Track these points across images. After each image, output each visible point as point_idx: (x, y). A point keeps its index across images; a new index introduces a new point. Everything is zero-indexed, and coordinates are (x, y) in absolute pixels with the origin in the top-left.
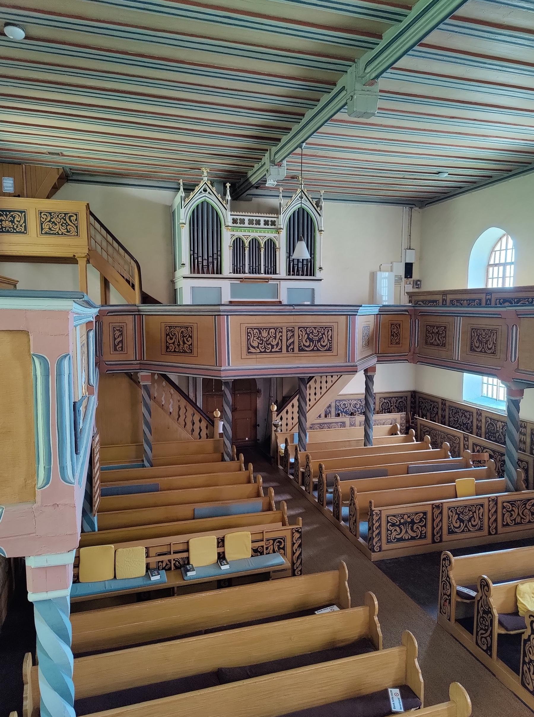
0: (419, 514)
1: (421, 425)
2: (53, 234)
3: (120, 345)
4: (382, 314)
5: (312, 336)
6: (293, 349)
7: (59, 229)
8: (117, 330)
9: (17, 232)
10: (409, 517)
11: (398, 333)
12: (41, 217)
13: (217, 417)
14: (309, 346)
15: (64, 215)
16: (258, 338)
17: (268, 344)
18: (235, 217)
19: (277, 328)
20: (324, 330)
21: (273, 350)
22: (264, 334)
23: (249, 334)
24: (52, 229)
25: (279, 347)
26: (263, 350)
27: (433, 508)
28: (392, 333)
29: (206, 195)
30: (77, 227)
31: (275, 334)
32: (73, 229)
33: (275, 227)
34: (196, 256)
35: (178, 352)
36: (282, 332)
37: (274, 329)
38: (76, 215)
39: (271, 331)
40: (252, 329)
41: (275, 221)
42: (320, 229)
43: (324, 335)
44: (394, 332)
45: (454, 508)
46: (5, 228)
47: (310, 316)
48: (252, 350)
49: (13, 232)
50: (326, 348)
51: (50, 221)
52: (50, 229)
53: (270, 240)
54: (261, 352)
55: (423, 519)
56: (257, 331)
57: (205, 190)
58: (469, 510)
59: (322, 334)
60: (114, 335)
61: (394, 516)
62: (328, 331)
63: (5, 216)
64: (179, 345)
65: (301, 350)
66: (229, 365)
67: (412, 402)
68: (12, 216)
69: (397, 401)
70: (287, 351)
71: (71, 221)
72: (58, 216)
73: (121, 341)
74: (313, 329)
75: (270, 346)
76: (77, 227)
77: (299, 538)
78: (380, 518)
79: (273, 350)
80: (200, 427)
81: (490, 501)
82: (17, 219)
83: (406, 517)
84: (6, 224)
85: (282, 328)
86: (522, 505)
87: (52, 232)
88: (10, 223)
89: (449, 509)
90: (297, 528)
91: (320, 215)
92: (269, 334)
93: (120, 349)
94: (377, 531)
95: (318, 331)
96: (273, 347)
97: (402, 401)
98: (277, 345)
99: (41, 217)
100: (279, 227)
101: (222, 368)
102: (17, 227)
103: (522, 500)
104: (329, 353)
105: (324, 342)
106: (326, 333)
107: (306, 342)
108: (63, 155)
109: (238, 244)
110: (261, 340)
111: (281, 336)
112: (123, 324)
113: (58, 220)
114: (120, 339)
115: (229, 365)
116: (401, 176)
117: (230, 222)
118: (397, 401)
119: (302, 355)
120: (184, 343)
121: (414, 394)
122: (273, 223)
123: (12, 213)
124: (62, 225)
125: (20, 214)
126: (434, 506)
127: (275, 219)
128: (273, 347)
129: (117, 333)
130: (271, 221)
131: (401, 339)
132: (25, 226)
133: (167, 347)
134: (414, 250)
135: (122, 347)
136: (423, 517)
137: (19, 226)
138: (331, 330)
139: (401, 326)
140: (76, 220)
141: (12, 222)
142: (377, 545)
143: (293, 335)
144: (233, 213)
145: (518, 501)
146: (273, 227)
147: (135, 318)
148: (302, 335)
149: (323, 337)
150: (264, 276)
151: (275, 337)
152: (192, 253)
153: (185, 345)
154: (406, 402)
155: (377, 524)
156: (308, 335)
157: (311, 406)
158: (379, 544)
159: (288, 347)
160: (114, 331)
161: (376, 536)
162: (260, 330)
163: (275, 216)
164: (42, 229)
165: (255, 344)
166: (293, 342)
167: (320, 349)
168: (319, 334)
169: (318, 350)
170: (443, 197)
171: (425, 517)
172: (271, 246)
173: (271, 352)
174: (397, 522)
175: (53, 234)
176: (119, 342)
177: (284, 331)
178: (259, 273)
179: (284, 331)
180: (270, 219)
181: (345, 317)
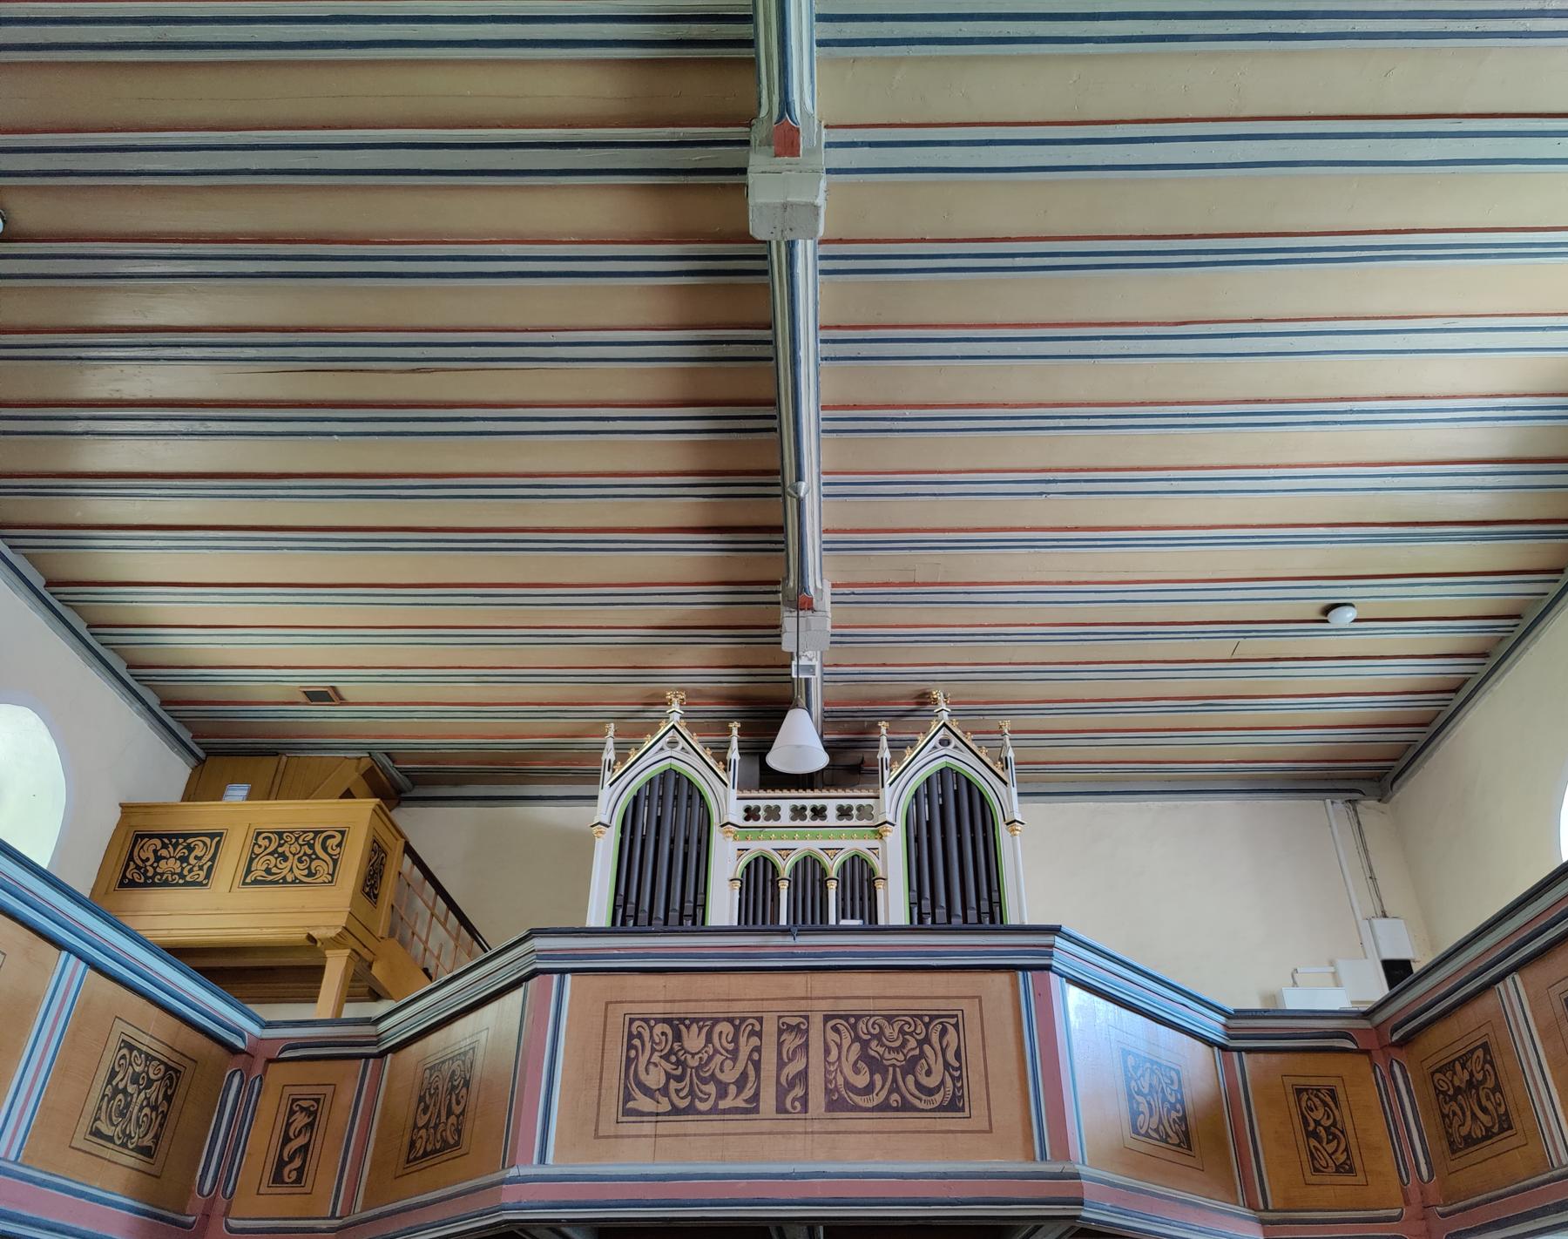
4: (1249, 1050)
6: (804, 1100)
8: (302, 1109)
9: (187, 884)
14: (869, 1089)
16: (666, 1058)
17: (705, 1081)
19: (743, 1020)
21: (723, 1105)
22: (694, 1041)
23: (636, 1042)
24: (274, 870)
25: (748, 1092)
30: (335, 862)
31: (735, 1040)
32: (323, 868)
36: (759, 1035)
37: (730, 1020)
38: (343, 833)
39: (718, 1029)
40: (646, 1021)
43: (926, 1047)
48: (642, 1102)
49: (177, 885)
50: (938, 1098)
51: (275, 851)
54: (675, 1111)
59: (920, 1043)
62: (944, 1032)
63: (171, 849)
70: (781, 1109)
71: (325, 848)
72: (297, 839)
73: (305, 1149)
75: (711, 1088)
79: (723, 1105)
88: (178, 863)
92: (709, 1040)
93: (294, 1175)
95: (901, 1031)
98: (741, 1082)
105: (929, 1073)
106: (935, 1038)
107: (857, 1071)
110: (678, 1063)
111: (758, 1049)
114: (301, 1141)
115: (542, 1160)
120: (450, 1113)
125: (207, 840)
129: (301, 1120)
132: (210, 869)
135: (300, 1170)
138: (956, 1026)
140: (339, 845)
141: (184, 859)
148: (839, 1047)
149: (922, 1055)
151: (734, 1054)
156: (865, 1045)
160: (292, 1113)
162: (677, 1025)
164: (249, 871)
165: (655, 1079)
167: (916, 1102)
169: (906, 1106)
170: (1422, 738)
173: (714, 1110)
175: (271, 882)
177: (770, 1028)
179: (770, 1028)
181: (1003, 979)
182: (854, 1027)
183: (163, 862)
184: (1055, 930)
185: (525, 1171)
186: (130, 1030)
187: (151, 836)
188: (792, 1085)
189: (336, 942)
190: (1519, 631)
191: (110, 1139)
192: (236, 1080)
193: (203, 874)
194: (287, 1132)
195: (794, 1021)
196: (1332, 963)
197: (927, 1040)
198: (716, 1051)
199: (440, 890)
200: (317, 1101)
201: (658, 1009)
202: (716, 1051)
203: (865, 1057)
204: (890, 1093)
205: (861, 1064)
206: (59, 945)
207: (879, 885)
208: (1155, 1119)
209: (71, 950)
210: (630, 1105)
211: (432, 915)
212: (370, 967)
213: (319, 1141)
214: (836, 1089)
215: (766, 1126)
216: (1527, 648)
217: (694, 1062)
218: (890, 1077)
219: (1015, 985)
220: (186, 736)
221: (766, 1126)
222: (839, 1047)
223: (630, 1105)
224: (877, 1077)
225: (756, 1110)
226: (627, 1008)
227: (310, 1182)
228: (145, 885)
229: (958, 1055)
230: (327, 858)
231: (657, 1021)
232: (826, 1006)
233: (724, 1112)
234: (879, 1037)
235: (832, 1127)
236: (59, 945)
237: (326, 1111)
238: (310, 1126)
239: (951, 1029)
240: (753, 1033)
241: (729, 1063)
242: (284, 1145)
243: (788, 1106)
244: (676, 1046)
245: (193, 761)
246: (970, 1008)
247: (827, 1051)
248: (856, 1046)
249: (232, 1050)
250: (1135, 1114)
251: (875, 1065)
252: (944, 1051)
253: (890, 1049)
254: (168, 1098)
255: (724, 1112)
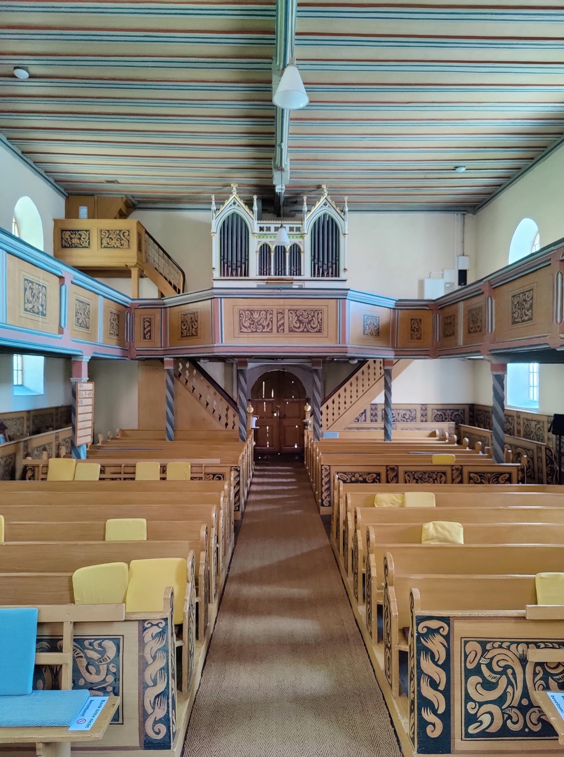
0: (372, 475)
1: (464, 432)
2: (110, 247)
3: (149, 334)
4: (401, 309)
5: (302, 318)
6: (283, 330)
7: (115, 243)
8: (147, 321)
9: (83, 247)
10: (360, 476)
11: (419, 328)
12: (101, 234)
13: (249, 413)
14: (299, 327)
15: (119, 232)
16: (249, 319)
17: (259, 325)
18: (262, 225)
19: (268, 311)
20: (314, 312)
21: (264, 330)
22: (256, 316)
23: (242, 316)
24: (110, 243)
25: (270, 328)
26: (254, 330)
27: (387, 470)
28: (412, 328)
29: (235, 208)
30: (129, 241)
31: (266, 315)
32: (125, 242)
33: (300, 233)
34: (225, 260)
35: (189, 336)
36: (272, 314)
37: (265, 311)
38: (128, 231)
39: (262, 312)
40: (244, 310)
41: (300, 228)
42: (344, 233)
43: (314, 318)
44: (415, 327)
45: (411, 472)
46: (74, 244)
47: (300, 300)
48: (244, 330)
49: (80, 247)
50: (316, 330)
51: (108, 237)
52: (108, 243)
53: (295, 245)
54: (252, 332)
55: (376, 480)
56: (249, 312)
57: (234, 203)
58: (428, 477)
59: (312, 317)
60: (144, 325)
61: (345, 473)
62: (318, 314)
63: (74, 235)
64: (189, 330)
65: (291, 331)
66: (222, 342)
67: (470, 416)
68: (80, 234)
69: (452, 413)
70: (278, 332)
71: (124, 236)
72: (114, 233)
73: (150, 331)
74: (303, 311)
75: (261, 327)
76: (129, 241)
77: (237, 476)
78: (329, 474)
79: (264, 330)
80: (234, 422)
81: (453, 470)
82: (83, 236)
83: (357, 475)
84: (75, 241)
85: (272, 311)
86: (494, 478)
87: (109, 246)
88: (78, 240)
89: (406, 473)
90: (236, 467)
91: (344, 220)
92: (260, 315)
93: (149, 337)
94: (327, 486)
95: (308, 314)
96: (264, 328)
97: (458, 414)
98: (268, 325)
99: (101, 234)
100: (303, 233)
101: (216, 345)
102: (83, 243)
103: (493, 473)
104: (318, 335)
105: (314, 324)
106: (316, 315)
107: (296, 323)
108: (118, 183)
109: (264, 250)
110: (252, 321)
111: (272, 318)
112: (151, 316)
113: (114, 236)
114: (149, 329)
115: (222, 342)
116: (423, 176)
117: (256, 229)
118: (452, 413)
119: (292, 336)
120: (193, 327)
121: (472, 407)
122: (298, 229)
123: (80, 232)
124: (117, 240)
125: (85, 232)
126: (388, 468)
127: (300, 226)
128: (264, 328)
129: (147, 324)
130: (296, 228)
131: (422, 334)
132: (89, 242)
133: (182, 333)
134: (468, 257)
135: (150, 336)
136: (376, 478)
137: (84, 242)
138: (321, 313)
139: (422, 322)
140: (129, 235)
141: (80, 239)
142: (326, 500)
143: (284, 317)
144: (259, 222)
145: (487, 473)
146: (298, 233)
147: (161, 310)
148: (292, 317)
149: (312, 319)
150: (288, 277)
151: (266, 318)
152: (222, 258)
153: (194, 329)
154: (464, 416)
155: (326, 479)
156: (298, 317)
157: (347, 408)
158: (328, 499)
159: (278, 328)
160: (144, 322)
161: (325, 491)
162: (252, 312)
163: (300, 222)
164: (102, 244)
165: (247, 324)
166: (283, 324)
167: (310, 331)
168: (308, 316)
169: (308, 331)
170: (488, 198)
171: (378, 478)
172: (296, 250)
173: (262, 332)
174: (347, 479)
175: (110, 247)
176: (148, 331)
177: (275, 313)
178: (285, 274)
179: (275, 313)
180: (295, 226)
181: (335, 300)
182: (296, 313)
183: (73, 240)
184: (349, 290)
185: (219, 345)
186: (111, 309)
187: (66, 231)
188: (280, 326)
189: (134, 267)
190: (519, 173)
191: (112, 334)
192: (129, 314)
193: (87, 244)
194: (144, 327)
195: (281, 311)
196: (443, 270)
197: (314, 316)
198: (261, 318)
199: (155, 241)
200: (150, 319)
201: (246, 308)
202: (261, 318)
203: (298, 320)
204: (304, 328)
205: (297, 322)
206: (98, 294)
207: (302, 255)
208: (370, 330)
209: (100, 295)
210: (241, 330)
211: (159, 255)
212: (143, 271)
213: (153, 328)
214: (291, 327)
215: (274, 335)
216: (520, 180)
217: (256, 321)
218: (304, 325)
219: (337, 303)
220: (62, 190)
221: (274, 335)
222: (292, 317)
223: (241, 330)
224: (301, 325)
225: (272, 332)
226: (238, 307)
227: (153, 338)
228: (69, 247)
229: (321, 320)
230: (126, 240)
231: (247, 310)
232: (289, 307)
233: (265, 332)
234: (302, 315)
235: (290, 336)
236: (98, 294)
237: (153, 321)
238: (150, 325)
239: (320, 313)
240: (270, 314)
241: (265, 321)
242: (144, 330)
243: (280, 331)
244: (252, 317)
245: (65, 198)
246: (325, 308)
247: (289, 319)
248: (296, 317)
249: (126, 307)
250: (364, 330)
251: (301, 322)
252: (318, 319)
253: (305, 318)
254: (118, 322)
255: (265, 332)
